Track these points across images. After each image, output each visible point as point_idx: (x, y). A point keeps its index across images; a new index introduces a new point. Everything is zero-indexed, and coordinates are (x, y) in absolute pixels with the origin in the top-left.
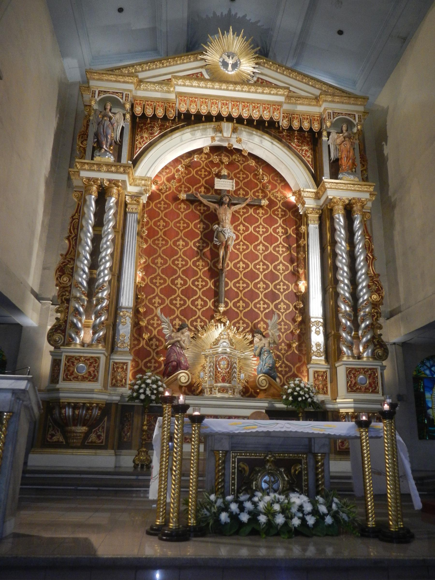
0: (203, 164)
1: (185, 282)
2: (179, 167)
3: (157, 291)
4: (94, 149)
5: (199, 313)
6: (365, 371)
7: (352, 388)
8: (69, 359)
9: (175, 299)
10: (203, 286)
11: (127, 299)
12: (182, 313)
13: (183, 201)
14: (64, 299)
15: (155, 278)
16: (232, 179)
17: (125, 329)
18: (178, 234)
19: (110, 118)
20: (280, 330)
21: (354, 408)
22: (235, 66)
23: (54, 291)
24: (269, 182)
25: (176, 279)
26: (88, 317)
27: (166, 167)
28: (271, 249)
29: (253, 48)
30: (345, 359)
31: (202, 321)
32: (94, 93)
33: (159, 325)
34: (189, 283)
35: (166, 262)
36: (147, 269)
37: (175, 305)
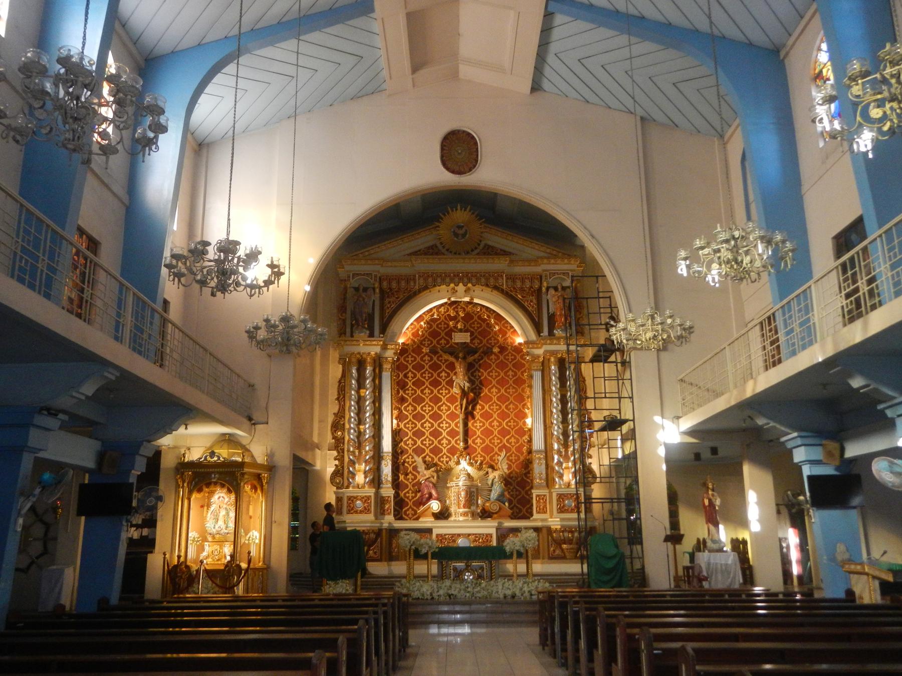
0: (442, 318)
1: (432, 425)
2: (422, 323)
3: (410, 434)
4: (352, 326)
5: (445, 451)
6: (571, 495)
7: (562, 510)
8: (349, 498)
9: (425, 440)
10: (447, 428)
11: (387, 444)
12: (432, 451)
13: (426, 354)
14: (338, 445)
15: (408, 423)
16: (466, 331)
17: (387, 469)
18: (424, 383)
19: (364, 299)
20: (511, 461)
21: (562, 526)
22: (464, 235)
23: (329, 440)
24: (500, 330)
25: (425, 423)
26: (360, 464)
27: (412, 324)
28: (503, 391)
29: (480, 219)
30: (557, 487)
31: (447, 457)
32: (349, 277)
33: (413, 463)
34: (436, 425)
35: (415, 409)
36: (400, 417)
37: (425, 445)
